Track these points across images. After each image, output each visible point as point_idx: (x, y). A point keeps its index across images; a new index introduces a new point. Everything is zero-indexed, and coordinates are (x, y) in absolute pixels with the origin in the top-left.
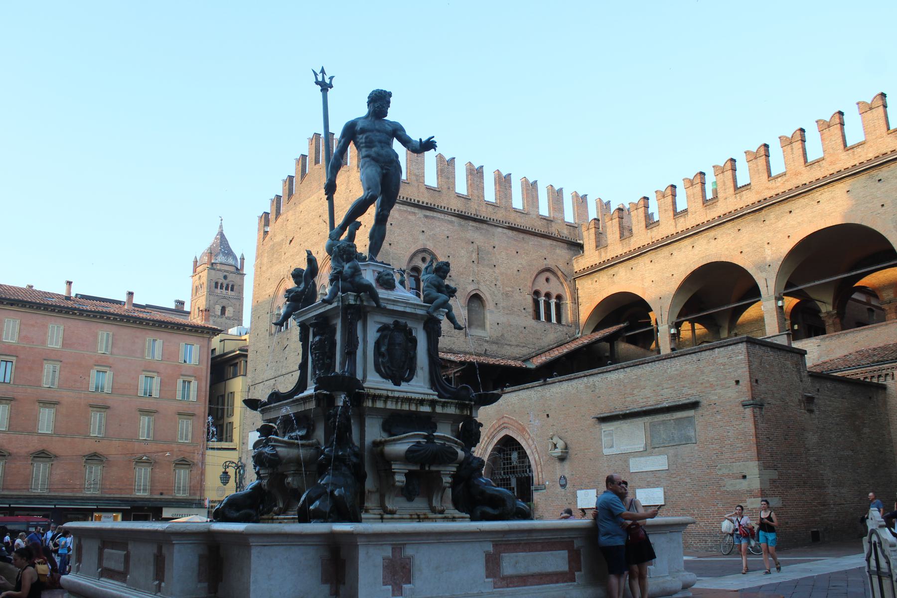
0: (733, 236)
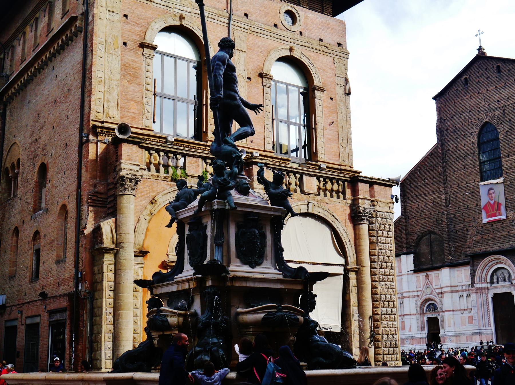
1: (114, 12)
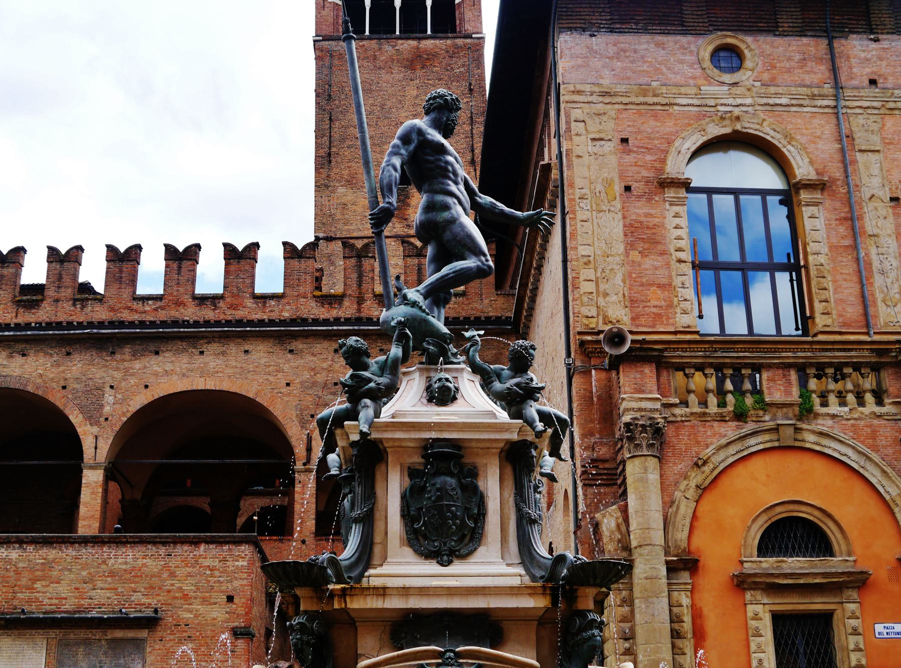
0: (55, 359)
1: (602, 139)
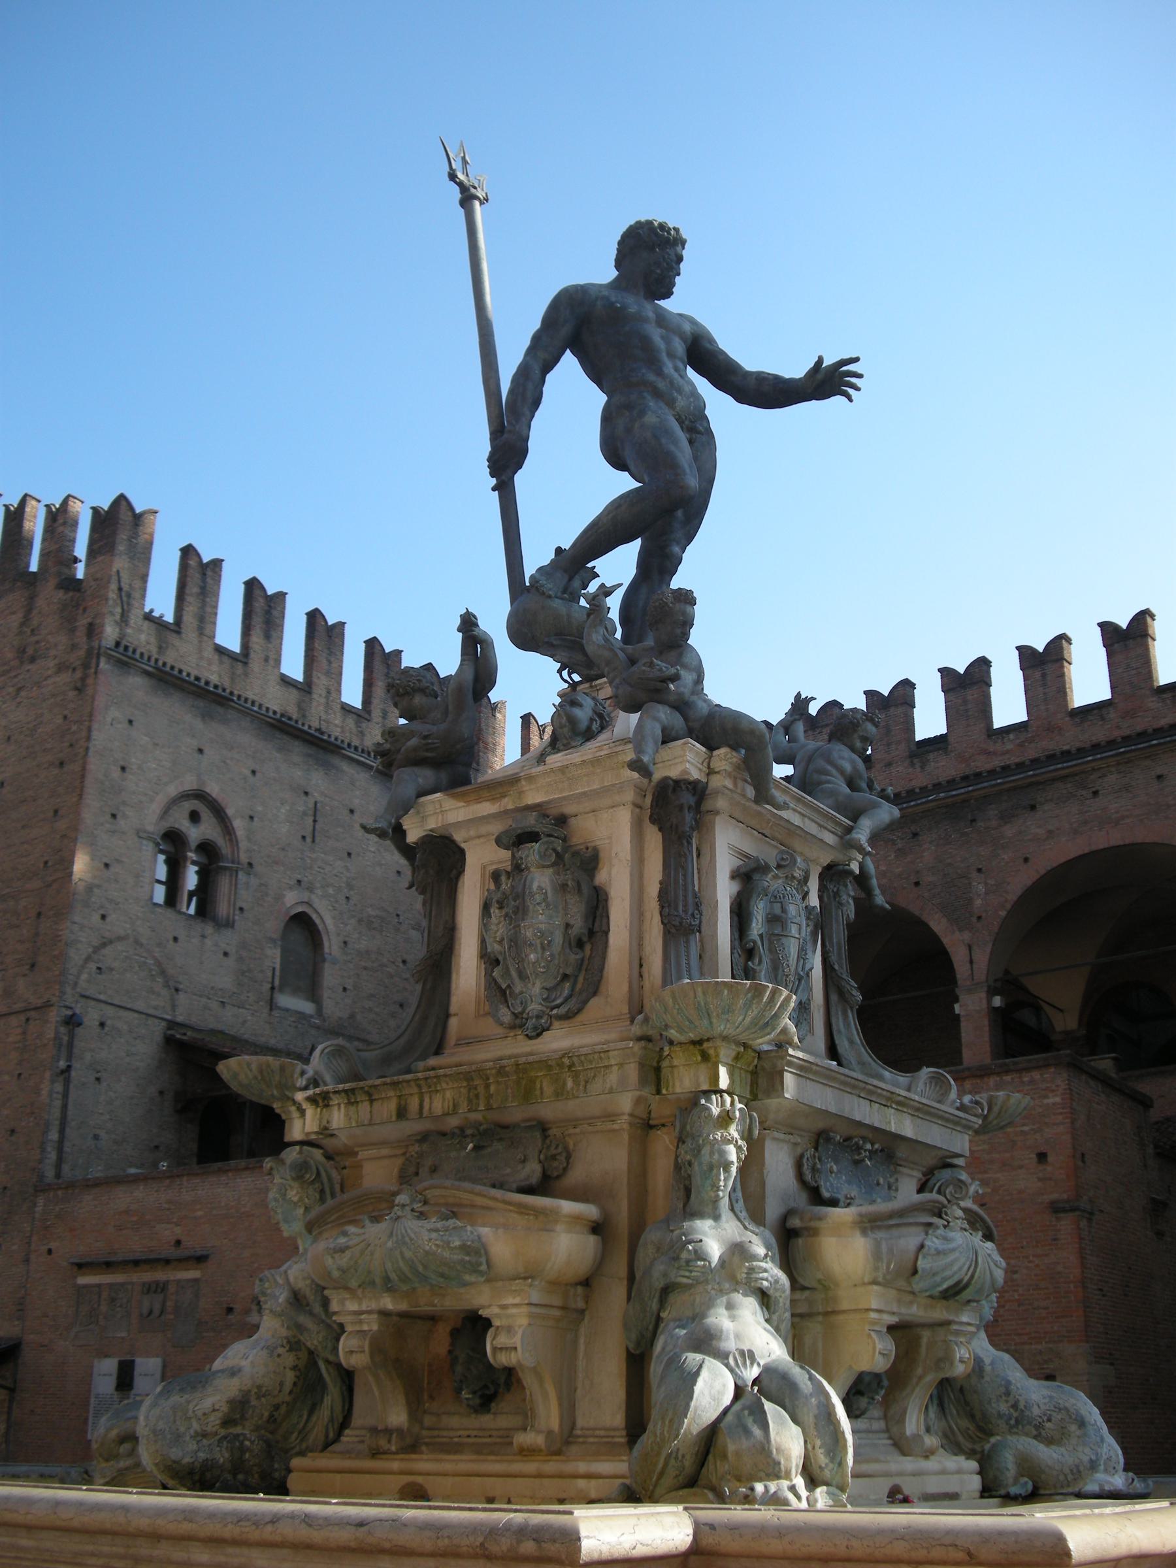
0: (900, 846)
